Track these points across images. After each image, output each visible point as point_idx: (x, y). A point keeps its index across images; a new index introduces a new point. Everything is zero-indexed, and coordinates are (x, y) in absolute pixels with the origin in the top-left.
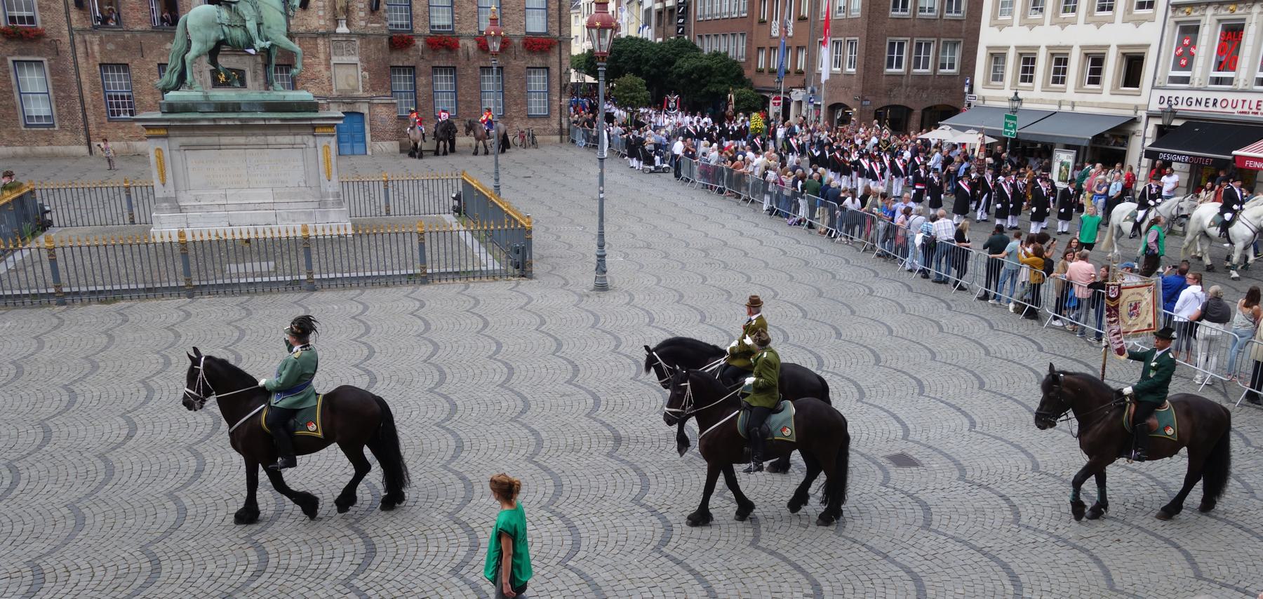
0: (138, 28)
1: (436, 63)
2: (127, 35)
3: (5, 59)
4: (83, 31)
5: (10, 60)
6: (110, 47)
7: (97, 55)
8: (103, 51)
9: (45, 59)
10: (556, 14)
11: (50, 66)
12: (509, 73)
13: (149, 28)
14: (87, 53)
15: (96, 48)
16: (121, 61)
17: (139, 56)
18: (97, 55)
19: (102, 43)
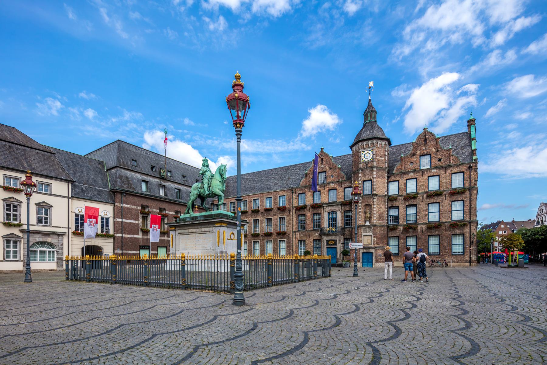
1: (408, 235)
4: (295, 232)
10: (468, 212)
12: (442, 237)
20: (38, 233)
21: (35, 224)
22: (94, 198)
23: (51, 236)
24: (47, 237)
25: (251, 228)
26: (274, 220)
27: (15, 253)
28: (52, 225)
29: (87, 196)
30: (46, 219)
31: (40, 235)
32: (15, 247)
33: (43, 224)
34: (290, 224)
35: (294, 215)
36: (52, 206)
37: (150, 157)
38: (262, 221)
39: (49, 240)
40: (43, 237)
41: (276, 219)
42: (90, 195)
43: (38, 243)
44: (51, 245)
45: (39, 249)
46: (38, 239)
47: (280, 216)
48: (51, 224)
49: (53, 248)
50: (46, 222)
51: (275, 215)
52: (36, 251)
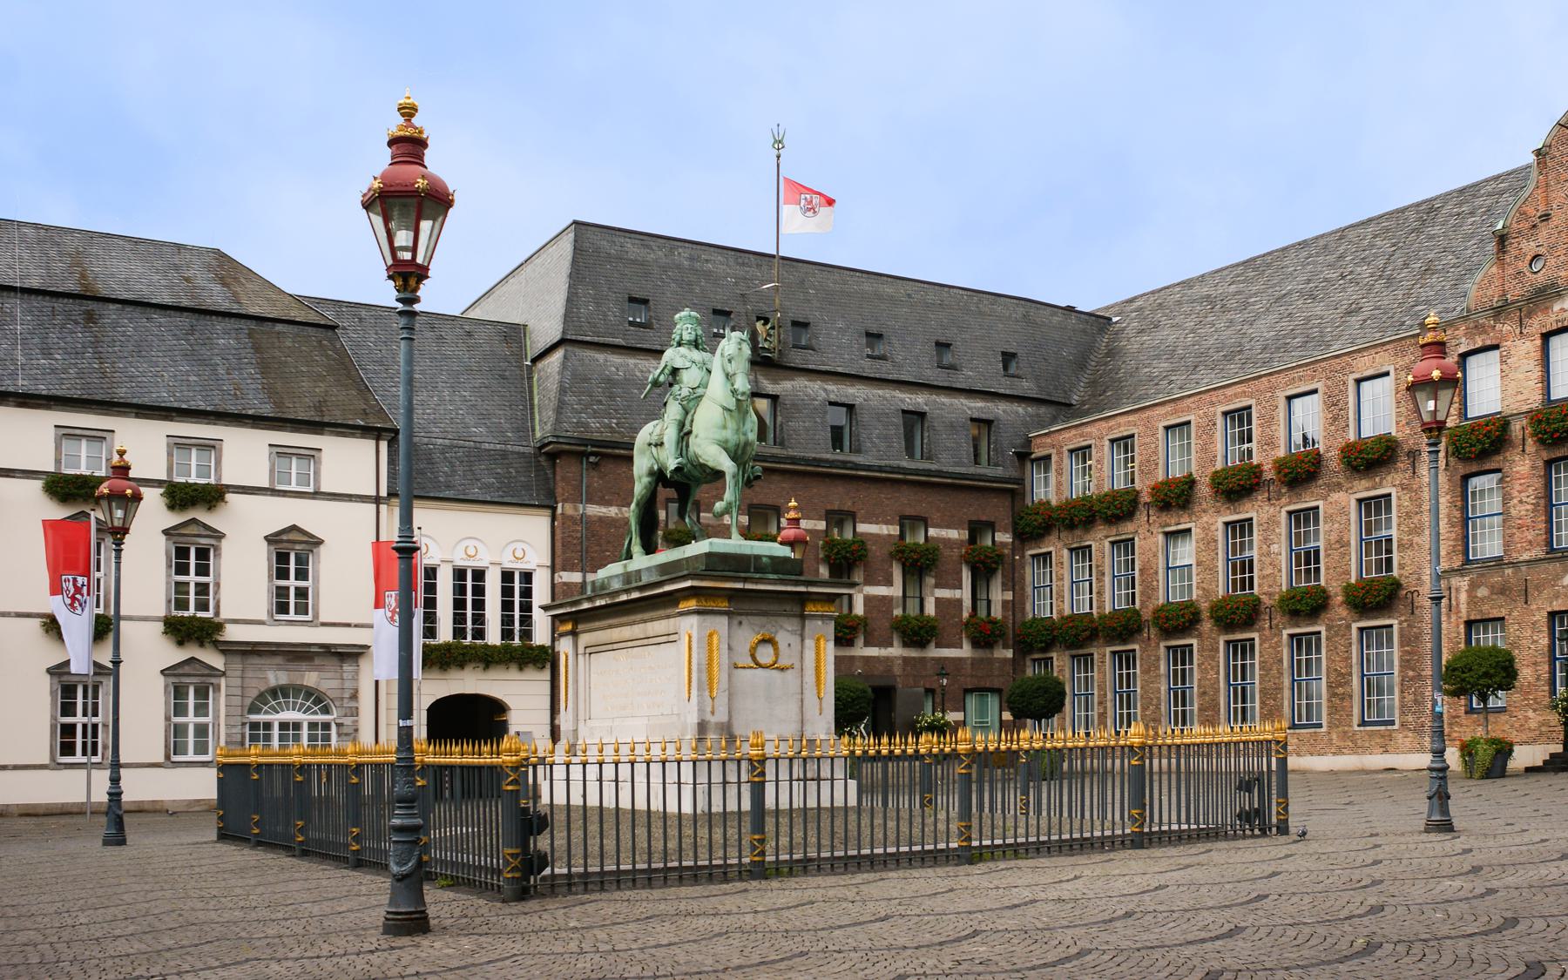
0: (1526, 556)
2: (1509, 571)
3: (1349, 627)
5: (1355, 626)
6: (1482, 592)
7: (1463, 608)
8: (1473, 600)
9: (1395, 622)
11: (1401, 630)
13: (1541, 555)
14: (1450, 606)
15: (1463, 597)
16: (1495, 614)
17: (1521, 604)
18: (1463, 608)
19: (1473, 586)
20: (274, 653)
21: (264, 617)
22: (475, 492)
23: (317, 661)
24: (304, 665)
25: (1212, 570)
26: (1329, 518)
27: (201, 731)
28: (322, 619)
29: (448, 487)
30: (302, 593)
31: (279, 660)
32: (201, 709)
33: (292, 616)
34: (1417, 530)
35: (1442, 478)
36: (319, 542)
37: (708, 275)
38: (1272, 522)
39: (311, 678)
40: (291, 666)
41: (1344, 511)
42: (457, 480)
43: (274, 692)
44: (318, 699)
45: (276, 718)
46: (276, 676)
47: (1364, 488)
48: (316, 616)
49: (326, 710)
50: (302, 609)
51: (1339, 486)
52: (268, 726)
